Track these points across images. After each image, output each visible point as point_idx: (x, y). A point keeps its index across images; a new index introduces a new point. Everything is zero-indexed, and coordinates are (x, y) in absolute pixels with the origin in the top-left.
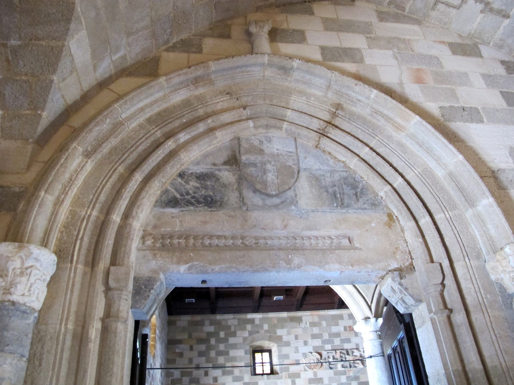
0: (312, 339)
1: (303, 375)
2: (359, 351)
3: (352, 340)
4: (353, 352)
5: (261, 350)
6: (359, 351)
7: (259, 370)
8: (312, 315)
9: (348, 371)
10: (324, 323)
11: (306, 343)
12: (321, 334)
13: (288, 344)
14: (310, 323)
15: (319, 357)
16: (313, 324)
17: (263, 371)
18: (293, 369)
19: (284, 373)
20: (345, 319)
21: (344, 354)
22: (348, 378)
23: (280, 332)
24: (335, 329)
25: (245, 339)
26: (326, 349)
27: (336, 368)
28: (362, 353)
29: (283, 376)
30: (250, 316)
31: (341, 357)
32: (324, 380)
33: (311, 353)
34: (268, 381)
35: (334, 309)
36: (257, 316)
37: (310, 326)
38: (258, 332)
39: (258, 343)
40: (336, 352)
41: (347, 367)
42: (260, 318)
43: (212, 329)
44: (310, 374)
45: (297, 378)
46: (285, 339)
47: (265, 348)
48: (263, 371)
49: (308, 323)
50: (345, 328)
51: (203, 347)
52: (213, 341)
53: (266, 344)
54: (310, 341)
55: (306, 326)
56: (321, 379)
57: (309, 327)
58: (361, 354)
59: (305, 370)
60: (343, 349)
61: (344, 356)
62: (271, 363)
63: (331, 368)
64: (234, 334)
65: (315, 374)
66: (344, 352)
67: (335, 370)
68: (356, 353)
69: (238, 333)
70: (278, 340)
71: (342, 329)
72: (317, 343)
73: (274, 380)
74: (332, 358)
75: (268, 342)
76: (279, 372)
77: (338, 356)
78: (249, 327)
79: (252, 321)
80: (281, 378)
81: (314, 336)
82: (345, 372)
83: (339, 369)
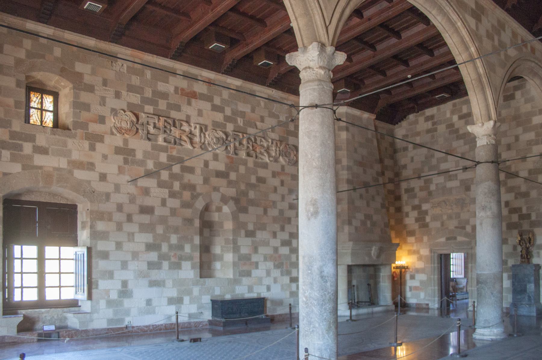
1: (108, 139)
2: (190, 125)
6: (190, 125)
9: (171, 148)
21: (169, 124)
22: (170, 158)
26: (146, 111)
27: (156, 140)
28: (193, 129)
31: (165, 127)
32: (137, 153)
34: (53, 136)
40: (159, 119)
41: (170, 143)
44: (118, 141)
45: (99, 142)
56: (134, 150)
58: (191, 130)
59: (112, 133)
60: (169, 118)
61: (169, 127)
63: (149, 139)
65: (126, 141)
66: (170, 121)
67: (154, 143)
68: (186, 127)
73: (63, 138)
74: (152, 125)
77: (161, 124)
82: (167, 147)
83: (159, 143)
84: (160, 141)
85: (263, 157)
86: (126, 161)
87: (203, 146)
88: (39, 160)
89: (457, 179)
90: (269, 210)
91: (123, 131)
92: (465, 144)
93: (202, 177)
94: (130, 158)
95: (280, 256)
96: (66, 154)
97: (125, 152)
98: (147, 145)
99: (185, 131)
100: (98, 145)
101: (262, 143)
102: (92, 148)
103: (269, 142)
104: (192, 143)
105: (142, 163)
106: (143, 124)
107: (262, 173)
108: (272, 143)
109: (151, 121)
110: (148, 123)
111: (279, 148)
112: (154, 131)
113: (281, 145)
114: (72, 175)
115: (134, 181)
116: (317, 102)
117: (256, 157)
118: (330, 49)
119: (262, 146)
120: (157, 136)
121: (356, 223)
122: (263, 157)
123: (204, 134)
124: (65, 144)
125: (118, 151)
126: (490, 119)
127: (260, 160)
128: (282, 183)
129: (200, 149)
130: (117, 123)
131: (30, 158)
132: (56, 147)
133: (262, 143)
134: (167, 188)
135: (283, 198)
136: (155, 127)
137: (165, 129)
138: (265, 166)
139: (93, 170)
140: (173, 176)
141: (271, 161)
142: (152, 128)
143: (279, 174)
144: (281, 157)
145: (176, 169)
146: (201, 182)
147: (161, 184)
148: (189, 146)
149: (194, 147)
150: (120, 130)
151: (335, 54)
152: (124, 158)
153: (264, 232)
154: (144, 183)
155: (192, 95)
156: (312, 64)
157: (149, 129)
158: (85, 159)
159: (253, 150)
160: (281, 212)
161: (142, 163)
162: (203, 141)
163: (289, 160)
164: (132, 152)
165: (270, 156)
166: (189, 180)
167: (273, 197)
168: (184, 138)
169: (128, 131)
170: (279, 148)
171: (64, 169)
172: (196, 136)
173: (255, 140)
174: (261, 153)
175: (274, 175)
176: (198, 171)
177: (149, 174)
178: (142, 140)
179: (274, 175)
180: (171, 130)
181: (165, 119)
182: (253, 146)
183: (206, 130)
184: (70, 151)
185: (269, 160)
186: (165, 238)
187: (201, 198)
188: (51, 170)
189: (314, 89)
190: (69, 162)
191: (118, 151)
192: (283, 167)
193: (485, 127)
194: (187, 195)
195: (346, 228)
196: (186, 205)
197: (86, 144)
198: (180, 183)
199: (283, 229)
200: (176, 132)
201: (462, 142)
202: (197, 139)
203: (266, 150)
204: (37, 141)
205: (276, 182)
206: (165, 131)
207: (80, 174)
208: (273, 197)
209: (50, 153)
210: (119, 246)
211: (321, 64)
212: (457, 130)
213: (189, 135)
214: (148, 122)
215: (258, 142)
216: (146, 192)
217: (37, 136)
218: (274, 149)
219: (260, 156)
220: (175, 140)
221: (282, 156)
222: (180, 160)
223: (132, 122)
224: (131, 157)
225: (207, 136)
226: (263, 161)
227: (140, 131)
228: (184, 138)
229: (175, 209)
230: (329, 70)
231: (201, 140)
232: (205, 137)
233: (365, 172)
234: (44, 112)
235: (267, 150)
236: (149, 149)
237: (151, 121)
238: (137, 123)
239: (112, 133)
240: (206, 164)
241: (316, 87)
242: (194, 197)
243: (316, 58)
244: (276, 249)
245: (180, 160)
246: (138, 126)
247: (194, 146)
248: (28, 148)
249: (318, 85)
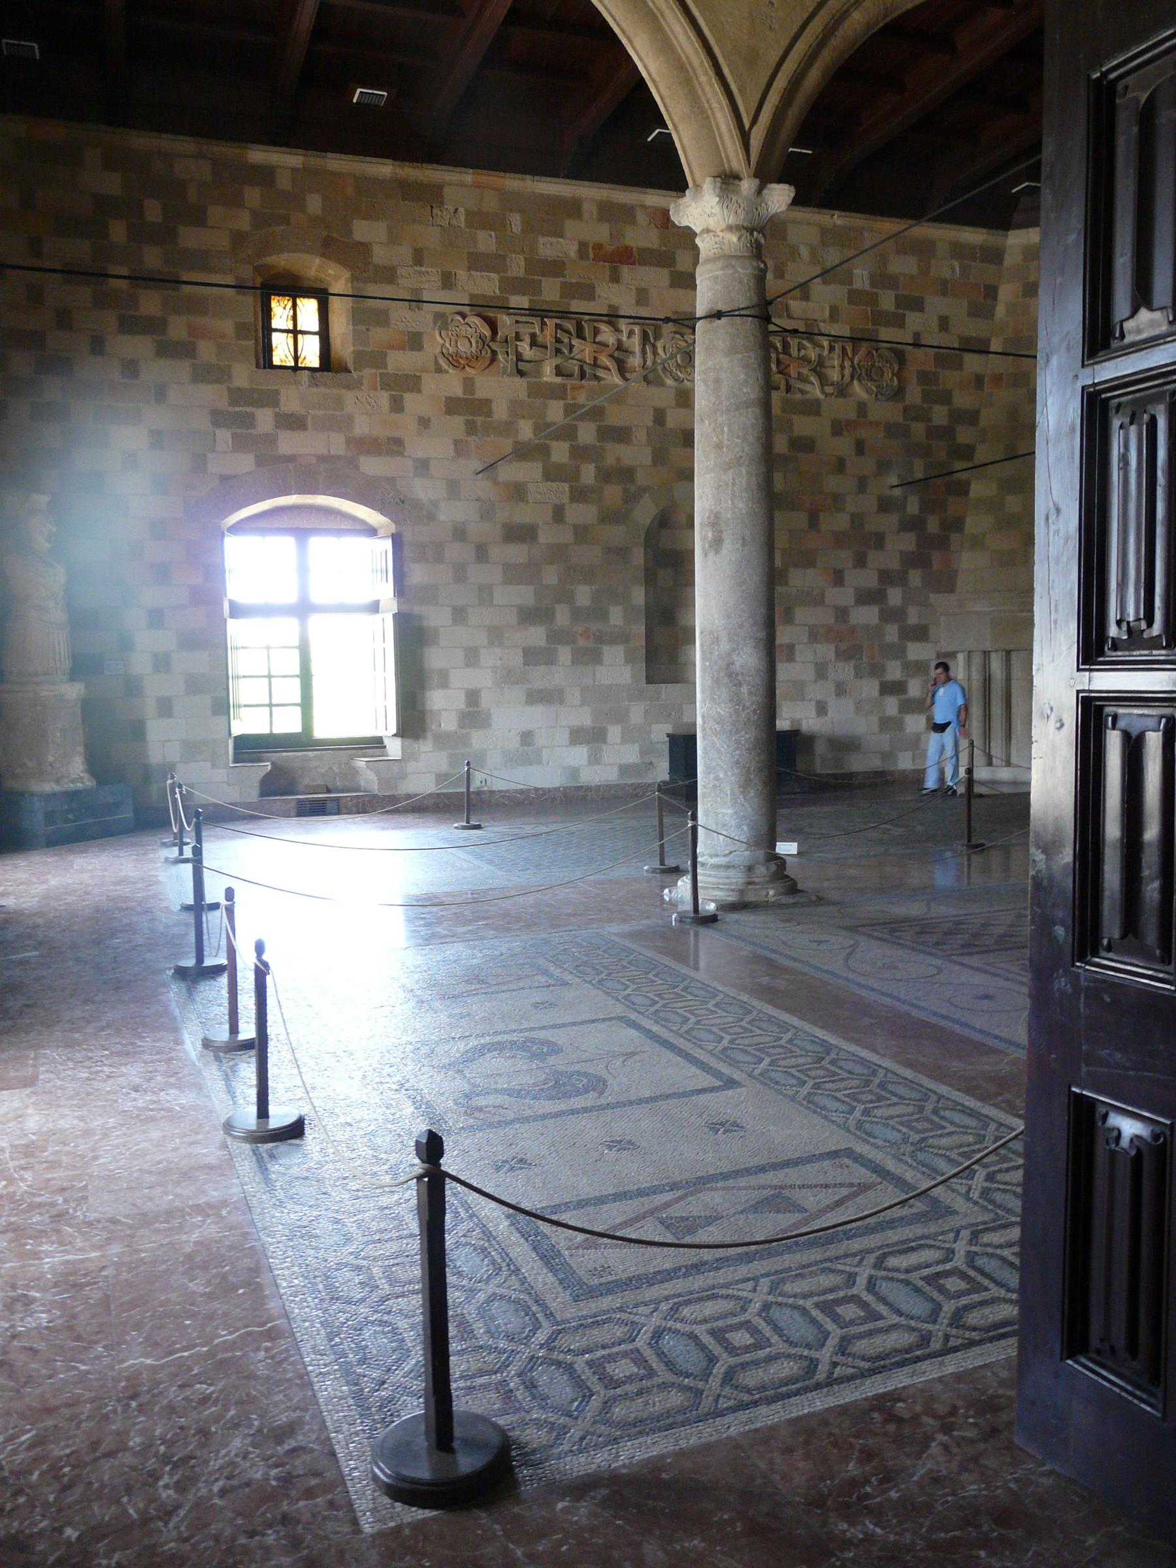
0: (470, 269)
1: (429, 383)
3: (598, 291)
4: (596, 331)
5: (295, 289)
6: (617, 330)
7: (282, 352)
8: (477, 186)
9: (573, 388)
10: (516, 222)
11: (448, 281)
12: (503, 258)
13: (388, 275)
14: (468, 213)
15: (487, 332)
16: (478, 219)
17: (296, 358)
18: (400, 361)
19: (367, 372)
20: (586, 216)
21: (568, 332)
22: (569, 410)
23: (364, 230)
24: (548, 247)
25: (239, 239)
27: (538, 373)
29: (365, 381)
30: (259, 155)
31: (558, 341)
32: (494, 407)
33: (464, 316)
35: (557, 176)
36: (286, 160)
37: (469, 224)
38: (286, 220)
39: (283, 261)
40: (543, 324)
41: (570, 376)
42: (294, 170)
43: (112, 184)
44: (452, 384)
46: (380, 255)
47: (307, 284)
48: (296, 358)
49: (461, 210)
50: (583, 246)
51: (80, 250)
52: (118, 232)
53: (313, 266)
54: (462, 274)
55: (454, 222)
56: (488, 402)
57: (463, 225)
58: (619, 341)
59: (439, 370)
61: (566, 340)
62: (324, 334)
63: (521, 373)
64: (198, 218)
66: (570, 326)
68: (607, 335)
69: (215, 213)
70: (355, 256)
71: (572, 250)
72: (487, 285)
73: (335, 391)
74: (527, 339)
75: (317, 261)
76: (351, 366)
77: (547, 337)
78: (253, 195)
79: (265, 176)
80: (357, 385)
81: (477, 262)
82: (564, 386)
84: (548, 375)
85: (807, 387)
86: (471, 428)
87: (651, 377)
88: (289, 443)
90: (822, 517)
91: (462, 362)
93: (649, 450)
94: (479, 420)
95: (853, 630)
96: (341, 423)
97: (468, 408)
98: (518, 387)
99: (605, 345)
100: (408, 397)
101: (803, 352)
102: (397, 406)
103: (823, 347)
104: (622, 370)
105: (508, 428)
106: (506, 341)
107: (803, 426)
108: (832, 349)
109: (525, 331)
110: (518, 337)
111: (852, 361)
112: (532, 353)
113: (854, 353)
114: (357, 467)
115: (490, 468)
117: (788, 389)
118: (748, 185)
119: (806, 360)
120: (537, 363)
122: (807, 387)
123: (654, 347)
124: (339, 403)
125: (453, 406)
127: (798, 396)
128: (860, 448)
129: (644, 384)
130: (447, 345)
131: (270, 440)
132: (322, 412)
133: (803, 352)
134: (565, 482)
135: (862, 485)
136: (534, 343)
137: (558, 346)
138: (812, 409)
139: (401, 454)
140: (580, 453)
141: (827, 395)
142: (528, 348)
143: (850, 425)
144: (855, 382)
145: (587, 433)
146: (648, 460)
147: (552, 474)
148: (617, 380)
149: (626, 379)
150: (455, 361)
151: (765, 192)
152: (467, 422)
153: (810, 572)
154: (512, 472)
155: (623, 257)
156: (712, 223)
157: (520, 349)
158: (380, 432)
159: (780, 372)
160: (857, 520)
161: (508, 428)
162: (649, 363)
163: (878, 387)
164: (483, 407)
165: (823, 381)
166: (618, 459)
167: (833, 483)
168: (604, 360)
169: (472, 359)
170: (852, 361)
171: (339, 457)
172: (633, 353)
173: (786, 346)
174: (801, 378)
175: (838, 428)
176: (640, 436)
177: (523, 452)
178: (506, 379)
179: (838, 428)
180: (571, 347)
181: (558, 321)
182: (779, 363)
183: (657, 336)
184: (350, 419)
185: (823, 392)
186: (566, 596)
187: (647, 499)
188: (314, 460)
189: (716, 278)
190: (350, 441)
191: (453, 406)
192: (862, 408)
194: (613, 493)
196: (610, 517)
197: (384, 398)
198: (597, 467)
199: (861, 562)
200: (584, 350)
202: (635, 361)
203: (814, 370)
204: (282, 403)
205: (843, 446)
206: (558, 351)
207: (372, 466)
208: (833, 483)
209: (309, 425)
210: (459, 615)
211: (732, 220)
213: (616, 354)
214: (517, 333)
215: (794, 351)
216: (518, 492)
217: (283, 392)
218: (836, 363)
219: (799, 385)
220: (581, 367)
221: (859, 380)
222: (596, 413)
223: (481, 338)
224: (482, 418)
225: (660, 351)
226: (806, 397)
227: (500, 357)
228: (604, 360)
229: (586, 528)
230: (751, 230)
231: (645, 362)
232: (655, 353)
234: (300, 336)
235: (819, 368)
236: (523, 395)
237: (525, 331)
238: (493, 339)
239: (439, 370)
240: (660, 416)
241: (720, 273)
242: (631, 498)
243: (717, 210)
244: (842, 613)
245: (596, 413)
246: (494, 346)
247: (627, 375)
248: (265, 419)
249: (723, 269)
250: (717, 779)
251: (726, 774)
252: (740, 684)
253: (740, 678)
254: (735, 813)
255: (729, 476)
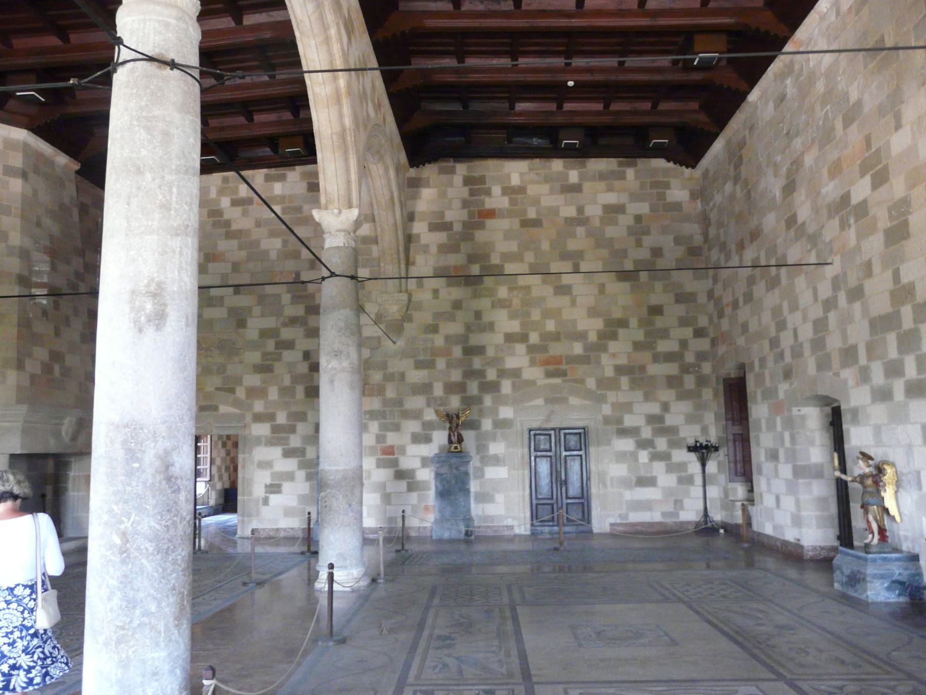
89: (222, 306)
92: (240, 248)
116: (171, 56)
121: (33, 367)
126: (350, 206)
189: (167, 25)
193: (343, 217)
195: (12, 376)
201: (234, 243)
212: (228, 224)
233: (54, 268)
241: (173, 21)
250: (147, 614)
251: (159, 605)
252: (178, 491)
253: (179, 482)
254: (169, 655)
255: (176, 243)
